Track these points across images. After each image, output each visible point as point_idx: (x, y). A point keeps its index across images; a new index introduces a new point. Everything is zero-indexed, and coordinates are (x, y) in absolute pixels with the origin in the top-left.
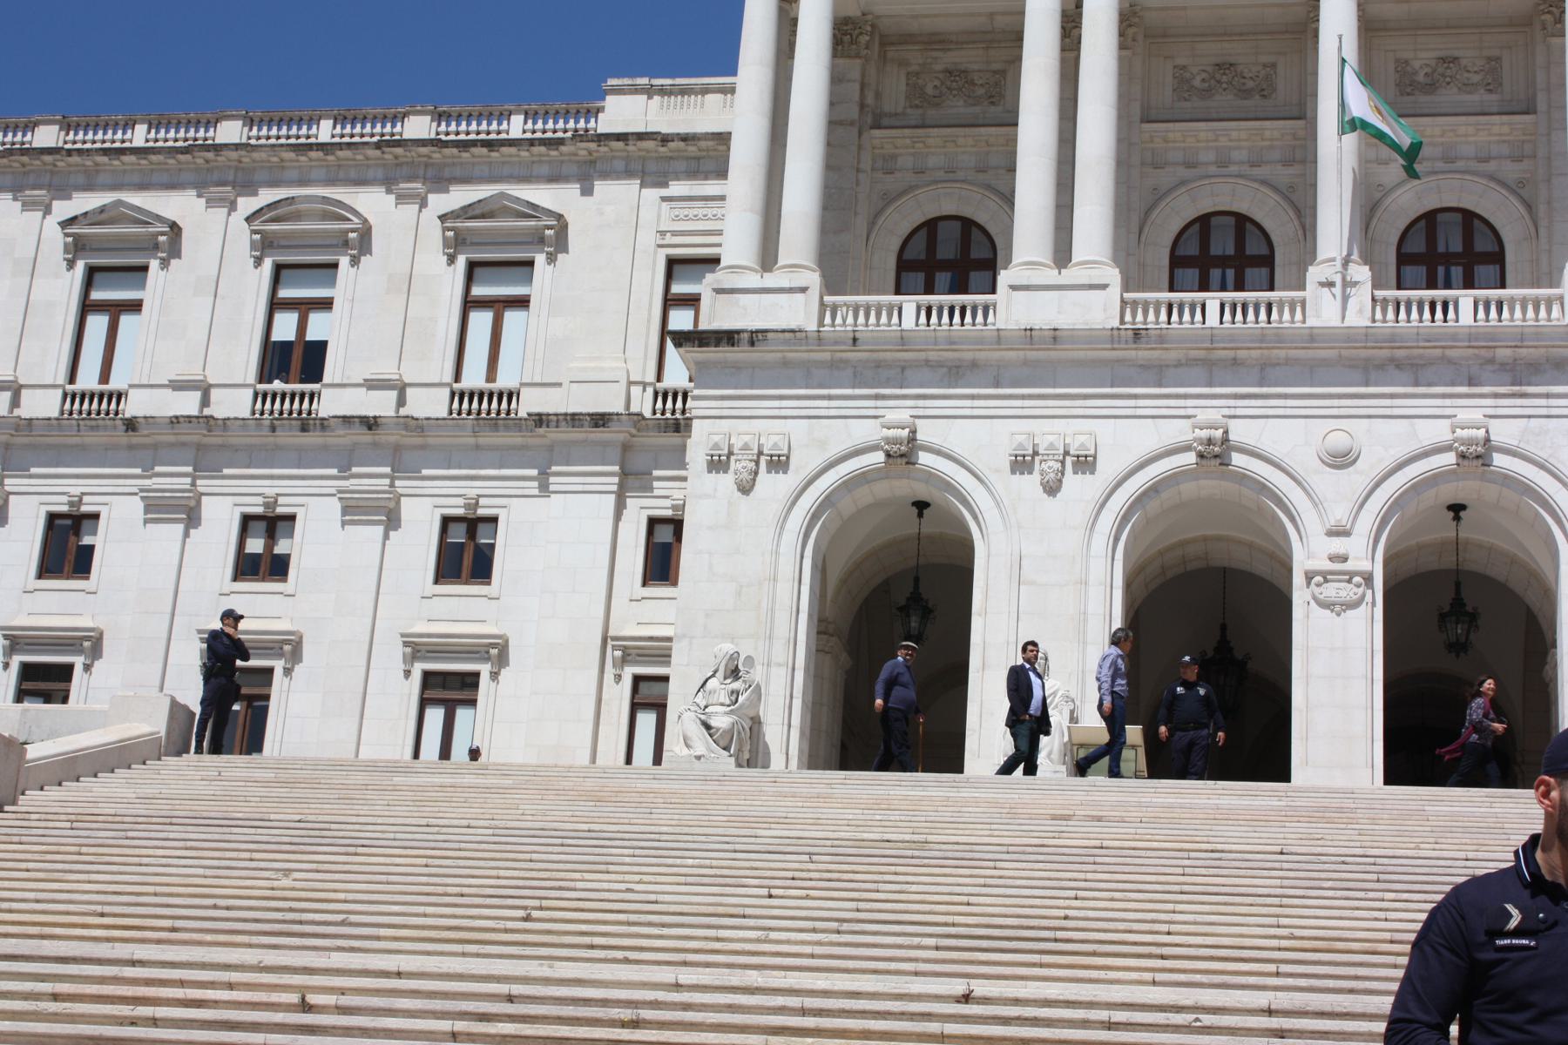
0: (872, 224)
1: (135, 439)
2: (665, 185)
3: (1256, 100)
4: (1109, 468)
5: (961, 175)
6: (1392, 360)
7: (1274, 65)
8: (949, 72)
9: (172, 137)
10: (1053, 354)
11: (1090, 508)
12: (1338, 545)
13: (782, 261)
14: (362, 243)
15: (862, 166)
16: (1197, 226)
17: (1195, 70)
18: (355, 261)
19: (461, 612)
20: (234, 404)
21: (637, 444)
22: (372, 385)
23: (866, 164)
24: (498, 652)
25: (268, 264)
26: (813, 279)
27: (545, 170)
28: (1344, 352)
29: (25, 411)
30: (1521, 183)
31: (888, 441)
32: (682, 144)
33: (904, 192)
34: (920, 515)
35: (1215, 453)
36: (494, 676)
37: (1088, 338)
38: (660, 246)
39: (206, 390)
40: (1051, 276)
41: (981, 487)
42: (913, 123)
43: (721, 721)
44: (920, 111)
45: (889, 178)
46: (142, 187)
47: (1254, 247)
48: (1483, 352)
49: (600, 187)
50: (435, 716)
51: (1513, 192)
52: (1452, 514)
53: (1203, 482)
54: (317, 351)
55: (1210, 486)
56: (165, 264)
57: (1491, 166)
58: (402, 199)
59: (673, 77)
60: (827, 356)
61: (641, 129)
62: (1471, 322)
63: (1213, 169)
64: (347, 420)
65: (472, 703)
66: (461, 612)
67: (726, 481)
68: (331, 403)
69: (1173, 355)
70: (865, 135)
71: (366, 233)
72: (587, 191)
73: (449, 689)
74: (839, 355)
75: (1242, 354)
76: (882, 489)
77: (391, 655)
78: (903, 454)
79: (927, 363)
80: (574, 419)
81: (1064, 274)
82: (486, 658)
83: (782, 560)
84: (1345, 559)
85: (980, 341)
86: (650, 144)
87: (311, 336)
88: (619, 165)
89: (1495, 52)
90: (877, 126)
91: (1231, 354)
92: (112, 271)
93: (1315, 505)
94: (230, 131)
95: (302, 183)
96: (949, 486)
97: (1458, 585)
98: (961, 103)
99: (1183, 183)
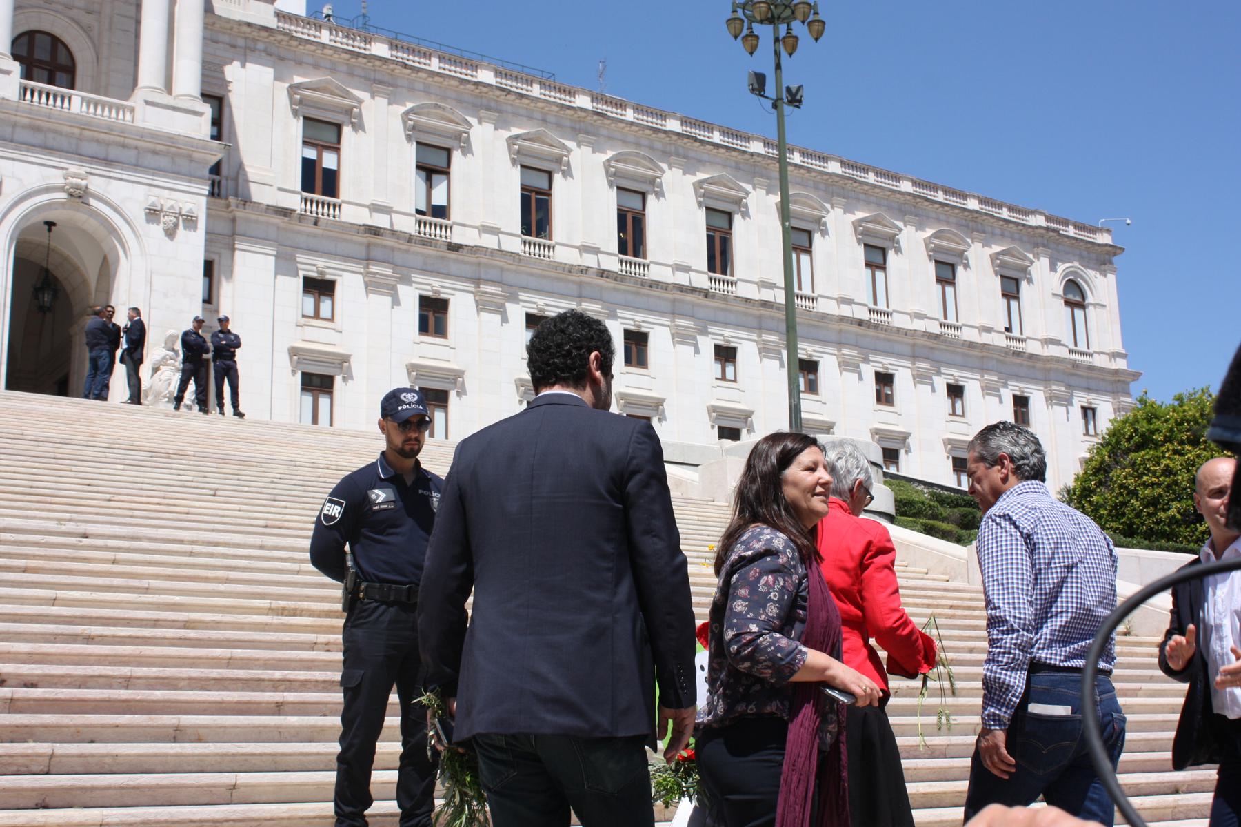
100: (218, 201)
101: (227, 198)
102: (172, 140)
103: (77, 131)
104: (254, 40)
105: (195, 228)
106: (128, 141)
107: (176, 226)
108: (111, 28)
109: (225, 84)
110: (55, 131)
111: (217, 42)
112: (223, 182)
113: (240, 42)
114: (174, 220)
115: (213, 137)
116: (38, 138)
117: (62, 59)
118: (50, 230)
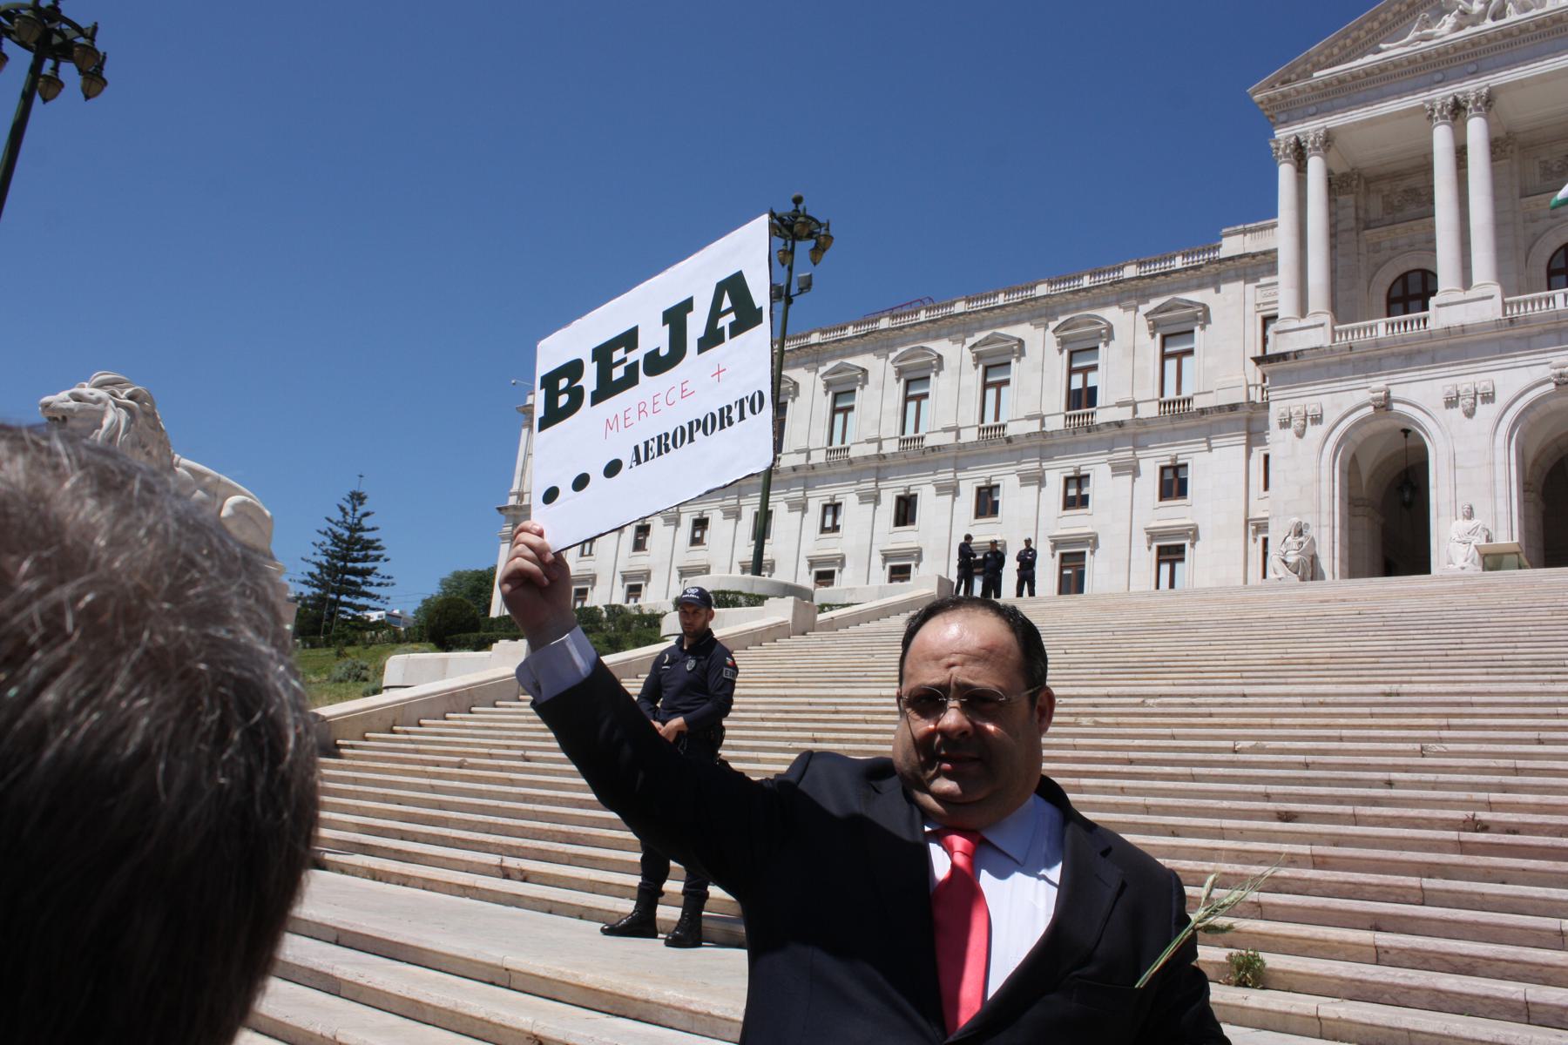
0: (1370, 282)
1: (1012, 446)
2: (1257, 280)
4: (1502, 398)
9: (1016, 297)
11: (1493, 422)
13: (1311, 310)
14: (1109, 334)
18: (1107, 344)
19: (1174, 514)
20: (1056, 423)
21: (1248, 421)
22: (1120, 405)
24: (1193, 533)
25: (1066, 352)
26: (1327, 318)
27: (1195, 282)
29: (1048, 428)
31: (1374, 400)
33: (1385, 262)
36: (1193, 545)
37: (1484, 327)
39: (1042, 418)
40: (1460, 296)
43: (1292, 559)
46: (1005, 324)
49: (1223, 287)
50: (1165, 568)
54: (1092, 392)
56: (1018, 360)
58: (1126, 309)
64: (1108, 424)
65: (1182, 560)
66: (1174, 514)
67: (1290, 433)
68: (1102, 416)
69: (1535, 330)
71: (1110, 329)
72: (1218, 291)
73: (1170, 554)
76: (1377, 426)
77: (1141, 539)
78: (1384, 405)
79: (1393, 354)
80: (1220, 409)
81: (1468, 297)
82: (1187, 537)
85: (1421, 338)
87: (1090, 384)
88: (1232, 273)
90: (1367, 228)
92: (995, 368)
94: (1042, 290)
95: (1078, 309)
96: (1411, 420)
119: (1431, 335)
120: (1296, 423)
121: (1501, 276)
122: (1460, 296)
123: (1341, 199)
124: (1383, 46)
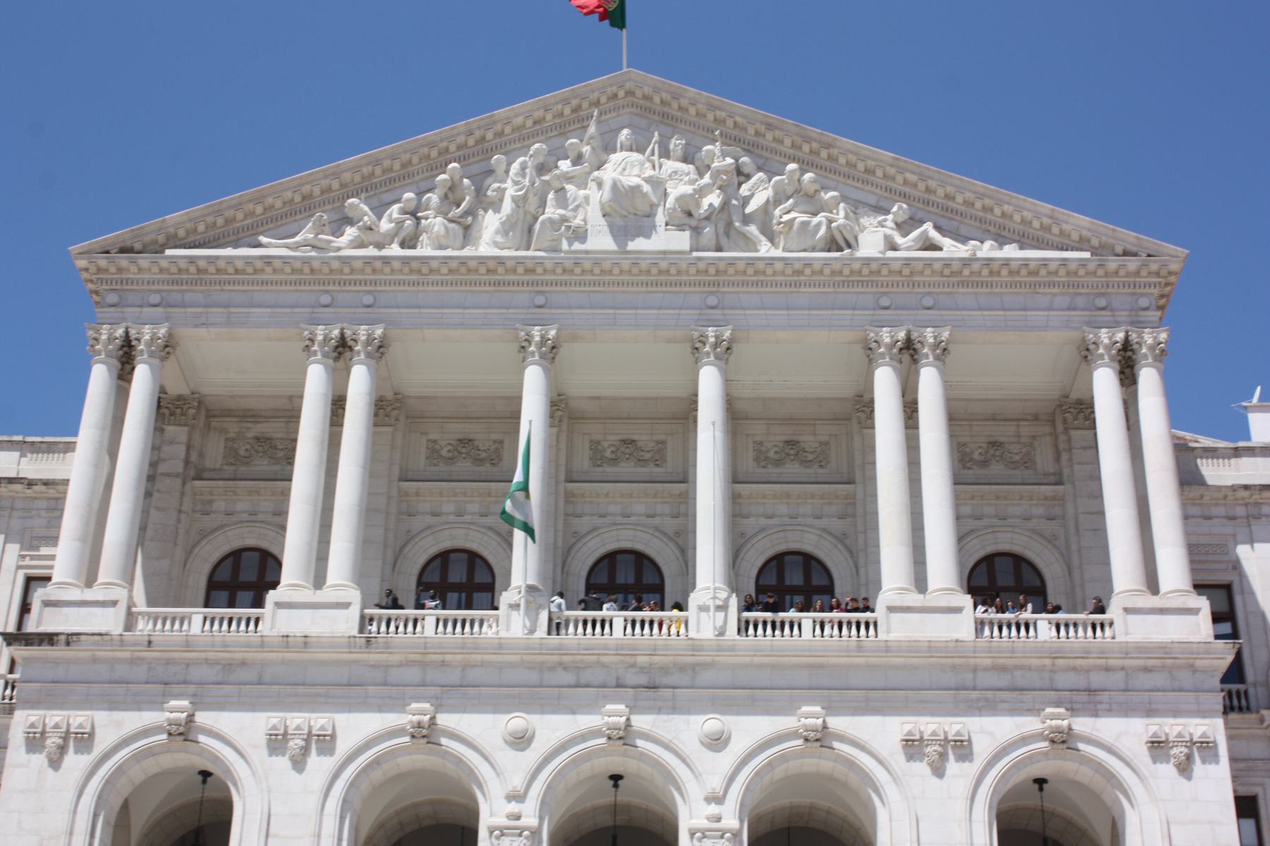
3: (486, 469)
4: (344, 745)
5: (261, 517)
6: (560, 664)
7: (501, 442)
8: (258, 439)
10: (305, 656)
12: (514, 807)
15: (184, 508)
16: (439, 560)
17: (443, 443)
23: (187, 506)
28: (525, 657)
30: (678, 534)
32: (44, 488)
33: (217, 529)
34: (204, 782)
35: (426, 734)
37: (331, 643)
38: (19, 567)
40: (308, 595)
41: (241, 761)
42: (227, 476)
44: (233, 468)
45: (206, 518)
47: (481, 577)
48: (628, 659)
51: (671, 539)
52: (612, 782)
53: (415, 757)
55: (422, 759)
57: (657, 521)
59: (43, 436)
60: (127, 655)
61: (13, 475)
62: (621, 635)
63: (452, 518)
70: (188, 486)
74: (137, 654)
75: (448, 657)
76: (167, 761)
78: (184, 732)
79: (207, 661)
83: (78, 817)
84: (518, 818)
85: (248, 645)
86: (18, 487)
89: (663, 437)
91: (439, 657)
93: (498, 775)
96: (216, 759)
97: (615, 837)
98: (265, 462)
99: (429, 527)
100: (1247, 716)
101: (1258, 712)
102: (1165, 650)
103: (1047, 662)
104: (1257, 504)
105: (1215, 758)
106: (1111, 662)
107: (1189, 758)
108: (1077, 531)
109: (1236, 566)
110: (1022, 668)
111: (1210, 518)
112: (1251, 691)
113: (1240, 511)
114: (1185, 750)
115: (1217, 637)
116: (1004, 680)
117: (1029, 579)
118: (1041, 789)
119: (263, 644)
120: (52, 741)
121: (360, 577)
122: (308, 595)
123: (171, 430)
124: (263, 239)
